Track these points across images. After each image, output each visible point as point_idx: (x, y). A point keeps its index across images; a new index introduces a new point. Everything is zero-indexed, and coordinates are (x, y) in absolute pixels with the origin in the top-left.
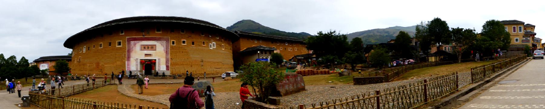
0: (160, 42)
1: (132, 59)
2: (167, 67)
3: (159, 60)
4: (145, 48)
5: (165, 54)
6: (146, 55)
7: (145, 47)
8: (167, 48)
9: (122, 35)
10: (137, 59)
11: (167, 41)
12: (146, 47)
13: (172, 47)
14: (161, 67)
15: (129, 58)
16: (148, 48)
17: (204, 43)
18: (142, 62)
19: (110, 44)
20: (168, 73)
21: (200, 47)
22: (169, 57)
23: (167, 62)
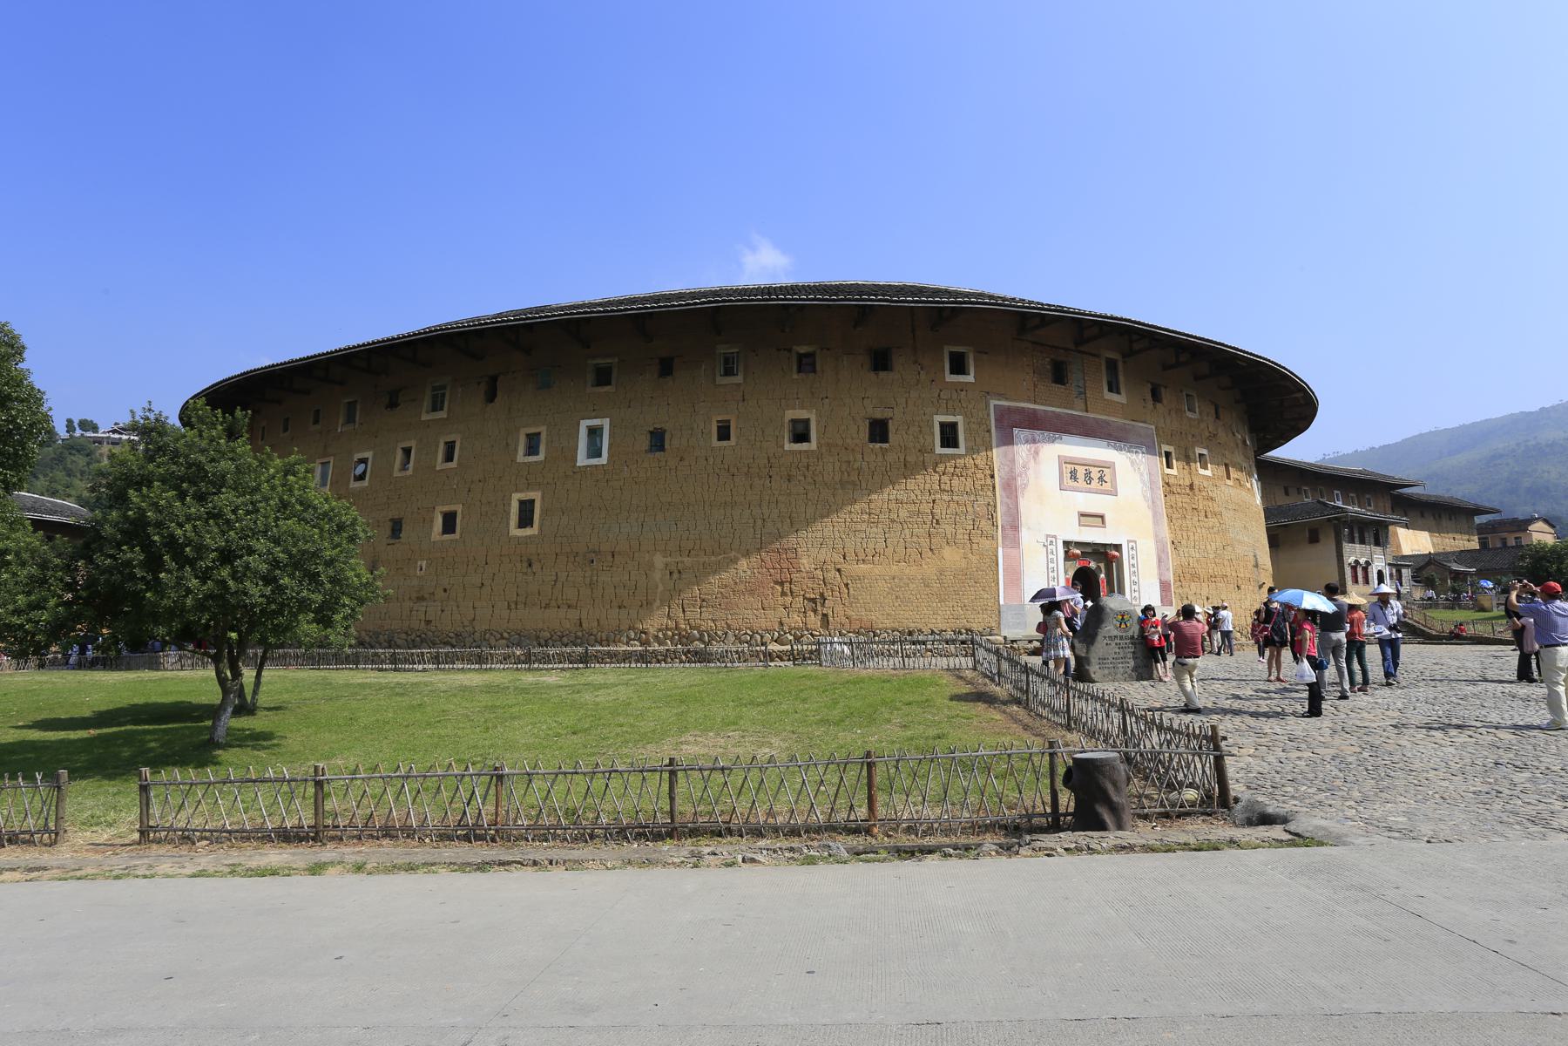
1: (1025, 534)
5: (1150, 514)
7: (1075, 474)
9: (963, 387)
10: (1052, 539)
15: (1014, 526)
19: (879, 431)
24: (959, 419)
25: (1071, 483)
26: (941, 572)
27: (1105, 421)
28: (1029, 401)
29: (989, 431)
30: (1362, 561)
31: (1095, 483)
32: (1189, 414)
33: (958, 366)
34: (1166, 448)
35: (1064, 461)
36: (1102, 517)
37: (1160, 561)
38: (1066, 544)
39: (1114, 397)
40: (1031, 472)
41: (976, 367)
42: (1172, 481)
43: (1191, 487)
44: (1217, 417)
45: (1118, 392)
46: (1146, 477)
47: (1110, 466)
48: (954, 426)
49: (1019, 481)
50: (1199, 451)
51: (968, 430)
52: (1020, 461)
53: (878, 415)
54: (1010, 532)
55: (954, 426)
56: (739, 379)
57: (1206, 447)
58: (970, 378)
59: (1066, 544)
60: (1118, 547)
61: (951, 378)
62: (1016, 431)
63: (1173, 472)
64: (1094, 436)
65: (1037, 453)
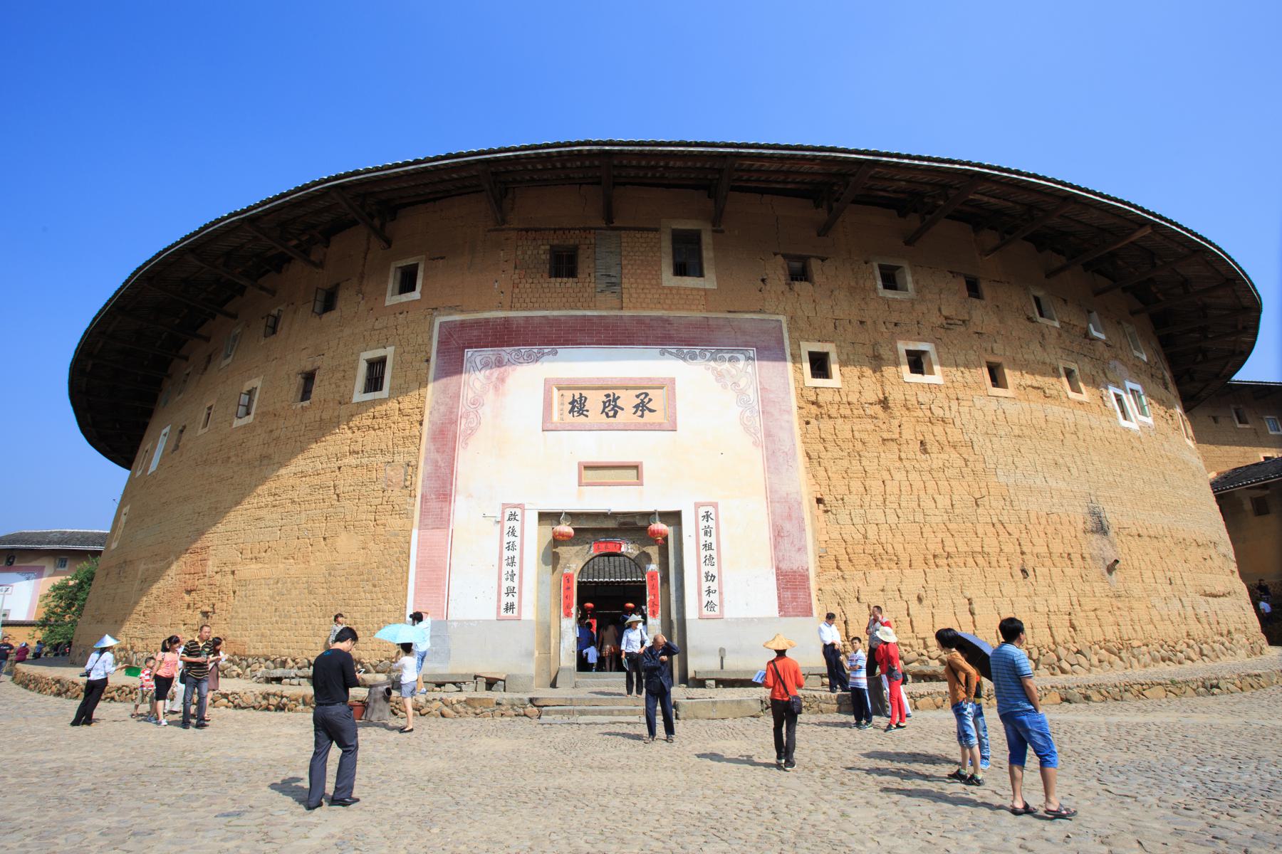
1: (462, 509)
2: (792, 588)
4: (578, 407)
5: (758, 455)
9: (401, 309)
15: (443, 492)
16: (611, 406)
21: (1055, 410)
22: (800, 484)
24: (389, 352)
26: (331, 570)
28: (501, 307)
29: (428, 361)
31: (626, 416)
32: (889, 294)
33: (407, 284)
36: (636, 467)
37: (778, 534)
38: (544, 517)
39: (689, 282)
40: (486, 411)
41: (425, 278)
43: (884, 403)
44: (974, 289)
45: (701, 275)
46: (752, 395)
47: (666, 385)
48: (382, 361)
49: (463, 425)
50: (902, 347)
51: (400, 364)
52: (467, 394)
53: (309, 368)
54: (434, 505)
55: (382, 361)
56: (229, 360)
57: (937, 341)
58: (416, 295)
60: (674, 518)
61: (393, 299)
62: (469, 353)
63: (835, 381)
65: (502, 380)
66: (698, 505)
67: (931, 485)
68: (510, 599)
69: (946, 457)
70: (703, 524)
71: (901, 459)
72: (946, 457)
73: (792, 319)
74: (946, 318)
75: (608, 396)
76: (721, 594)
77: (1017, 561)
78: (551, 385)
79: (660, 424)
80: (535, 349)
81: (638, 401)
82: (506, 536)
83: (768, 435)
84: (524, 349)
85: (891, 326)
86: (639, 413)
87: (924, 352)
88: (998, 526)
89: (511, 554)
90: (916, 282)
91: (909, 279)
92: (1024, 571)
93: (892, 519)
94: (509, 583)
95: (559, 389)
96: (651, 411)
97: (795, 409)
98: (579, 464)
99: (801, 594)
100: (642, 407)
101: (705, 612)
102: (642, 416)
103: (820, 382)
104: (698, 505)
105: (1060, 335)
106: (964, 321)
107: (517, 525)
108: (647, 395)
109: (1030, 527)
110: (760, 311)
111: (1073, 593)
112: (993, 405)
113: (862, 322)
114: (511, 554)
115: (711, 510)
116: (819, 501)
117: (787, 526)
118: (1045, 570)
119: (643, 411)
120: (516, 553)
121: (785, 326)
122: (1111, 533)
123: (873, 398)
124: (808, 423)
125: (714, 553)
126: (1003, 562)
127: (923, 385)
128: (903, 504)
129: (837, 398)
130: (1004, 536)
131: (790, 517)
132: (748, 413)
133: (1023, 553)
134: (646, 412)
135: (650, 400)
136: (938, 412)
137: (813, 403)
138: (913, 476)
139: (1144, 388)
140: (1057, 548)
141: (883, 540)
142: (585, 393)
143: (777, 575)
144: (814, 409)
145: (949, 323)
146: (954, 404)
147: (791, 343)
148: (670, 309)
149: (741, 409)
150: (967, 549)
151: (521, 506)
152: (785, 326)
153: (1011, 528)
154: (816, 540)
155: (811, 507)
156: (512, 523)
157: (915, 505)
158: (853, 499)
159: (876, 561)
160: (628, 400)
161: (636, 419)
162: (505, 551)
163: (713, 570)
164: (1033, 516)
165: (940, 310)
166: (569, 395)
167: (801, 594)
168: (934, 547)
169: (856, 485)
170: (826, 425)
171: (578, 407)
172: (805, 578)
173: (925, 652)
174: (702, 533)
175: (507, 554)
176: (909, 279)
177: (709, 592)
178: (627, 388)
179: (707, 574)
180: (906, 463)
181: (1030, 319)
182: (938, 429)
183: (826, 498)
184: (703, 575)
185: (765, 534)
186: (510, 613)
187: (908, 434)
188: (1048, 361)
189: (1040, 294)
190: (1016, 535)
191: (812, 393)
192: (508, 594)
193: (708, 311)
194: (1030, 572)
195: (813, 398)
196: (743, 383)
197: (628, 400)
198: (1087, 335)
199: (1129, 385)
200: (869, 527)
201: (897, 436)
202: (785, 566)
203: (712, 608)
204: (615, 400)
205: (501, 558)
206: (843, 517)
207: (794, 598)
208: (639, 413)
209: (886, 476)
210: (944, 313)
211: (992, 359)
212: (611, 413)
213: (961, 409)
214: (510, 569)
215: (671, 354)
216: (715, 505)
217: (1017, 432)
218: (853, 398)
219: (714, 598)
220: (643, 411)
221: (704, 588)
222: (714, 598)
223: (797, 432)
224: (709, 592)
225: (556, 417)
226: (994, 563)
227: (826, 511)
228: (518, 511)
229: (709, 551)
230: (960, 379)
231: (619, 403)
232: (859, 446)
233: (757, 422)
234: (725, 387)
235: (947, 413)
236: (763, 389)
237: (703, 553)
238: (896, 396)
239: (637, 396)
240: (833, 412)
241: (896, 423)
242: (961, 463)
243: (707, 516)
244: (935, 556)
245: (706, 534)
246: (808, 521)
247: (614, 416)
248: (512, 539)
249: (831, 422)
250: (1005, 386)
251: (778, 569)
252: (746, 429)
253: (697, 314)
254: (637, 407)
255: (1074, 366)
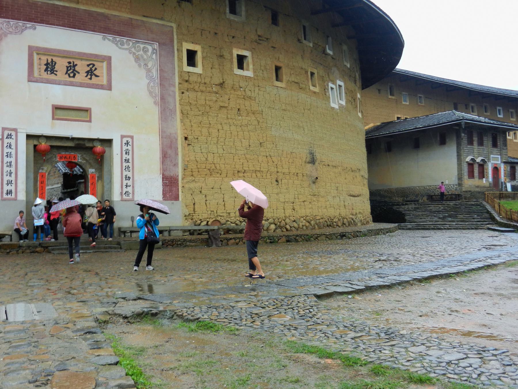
0: (128, 43)
3: (128, 141)
4: (50, 67)
5: (155, 111)
6: (59, 111)
7: (48, 66)
8: (164, 81)
11: (166, 44)
12: (61, 64)
13: (185, 80)
14: (136, 184)
16: (72, 70)
17: (312, 74)
18: (43, 149)
20: (174, 218)
21: (303, 96)
22: (178, 129)
23: (167, 156)
25: (45, 75)
27: (102, 14)
30: (479, 160)
31: (81, 77)
32: (232, 17)
34: (187, 46)
35: (32, 50)
37: (165, 156)
38: (29, 137)
42: (192, 79)
44: (275, 21)
46: (155, 73)
50: (236, 52)
57: (252, 50)
59: (29, 137)
60: (109, 142)
63: (198, 70)
64: (54, 25)
66: (122, 137)
67: (241, 133)
68: (9, 188)
69: (249, 119)
70: (125, 148)
71: (228, 118)
72: (249, 119)
73: (179, 26)
74: (259, 36)
75: (69, 63)
76: (133, 187)
77: (274, 177)
78: (32, 50)
79: (102, 85)
80: (21, 23)
81: (88, 69)
82: (5, 149)
83: (162, 98)
84: (12, 22)
85: (231, 38)
86: (89, 77)
87: (246, 57)
88: (269, 157)
89: (9, 160)
90: (247, 11)
91: (243, 8)
92: (277, 181)
93: (221, 151)
94: (8, 178)
95: (38, 54)
96: (96, 76)
97: (177, 84)
98: (53, 106)
99: (174, 189)
100: (91, 73)
101: (125, 197)
102: (91, 79)
103: (191, 69)
104: (122, 137)
105: (312, 51)
106: (267, 39)
107: (13, 142)
108: (94, 65)
109: (283, 159)
110: (162, 19)
111: (296, 193)
112: (275, 91)
113: (216, 33)
114: (9, 160)
115: (130, 140)
116: (186, 138)
117: (169, 152)
118: (286, 181)
119: (91, 75)
120: (13, 160)
121: (175, 30)
122: (317, 164)
123: (218, 82)
124: (183, 93)
125: (130, 165)
126: (268, 176)
127: (243, 76)
128: (227, 143)
129: (199, 80)
130: (270, 163)
131: (171, 147)
132: (152, 84)
133: (278, 172)
134: (93, 77)
135: (96, 69)
136: (249, 93)
137: (187, 81)
138: (233, 128)
139: (345, 84)
140: (293, 170)
141: (215, 162)
142: (55, 59)
143: (163, 178)
144: (186, 85)
145: (260, 39)
146: (257, 89)
147: (178, 42)
148: (108, 9)
149: (148, 81)
150: (254, 169)
151: (15, 130)
152: (175, 30)
153: (274, 159)
154: (183, 160)
155: (182, 142)
156: (9, 141)
157: (232, 144)
158: (202, 139)
159: (211, 172)
160: (82, 67)
161: (87, 81)
162: (5, 158)
163: (129, 174)
164: (285, 153)
165: (256, 31)
166: (44, 59)
167: (174, 189)
168: (239, 167)
169: (205, 131)
170: (192, 95)
171: (50, 67)
172: (177, 180)
173: (229, 219)
174: (124, 153)
175: (6, 160)
176: (243, 8)
177: (127, 186)
178: (82, 59)
179: (126, 176)
180: (230, 121)
181: (299, 40)
182: (247, 103)
183: (190, 137)
184: (124, 177)
185: (157, 155)
186: (9, 196)
187: (232, 104)
188: (304, 67)
189: (307, 24)
190: (276, 163)
191: (187, 75)
192: (8, 184)
193: (132, 14)
194: (280, 182)
195: (187, 79)
196: (150, 65)
197: (82, 67)
198: (324, 52)
199: (339, 82)
200: (209, 154)
201: (226, 105)
202: (167, 173)
203: (128, 195)
204: (75, 66)
205: (2, 162)
206: (197, 149)
207: (171, 191)
208: (89, 77)
209: (220, 127)
210: (259, 33)
211: (279, 64)
212: (72, 75)
213: (260, 93)
214: (8, 169)
215: (109, 40)
216: (132, 137)
217: (284, 107)
218: (207, 80)
219: (130, 189)
220: (91, 75)
221: (124, 184)
222: (130, 189)
223: (178, 98)
224: (127, 186)
225: (36, 74)
226: (265, 177)
227: (189, 145)
228: (13, 133)
229: (128, 164)
230: (261, 75)
231: (77, 68)
232: (208, 108)
233: (157, 90)
234: (140, 66)
235: (253, 94)
236: (161, 70)
237: (125, 164)
238: (229, 82)
239: (88, 65)
240: (196, 88)
241: (227, 97)
242: (256, 123)
243: (127, 143)
244: (238, 172)
245: (126, 153)
246: (180, 150)
247: (74, 76)
248: (9, 150)
249: (195, 94)
250: (281, 81)
251: (163, 175)
252: (151, 93)
253: (126, 15)
254: (87, 72)
255: (315, 71)
